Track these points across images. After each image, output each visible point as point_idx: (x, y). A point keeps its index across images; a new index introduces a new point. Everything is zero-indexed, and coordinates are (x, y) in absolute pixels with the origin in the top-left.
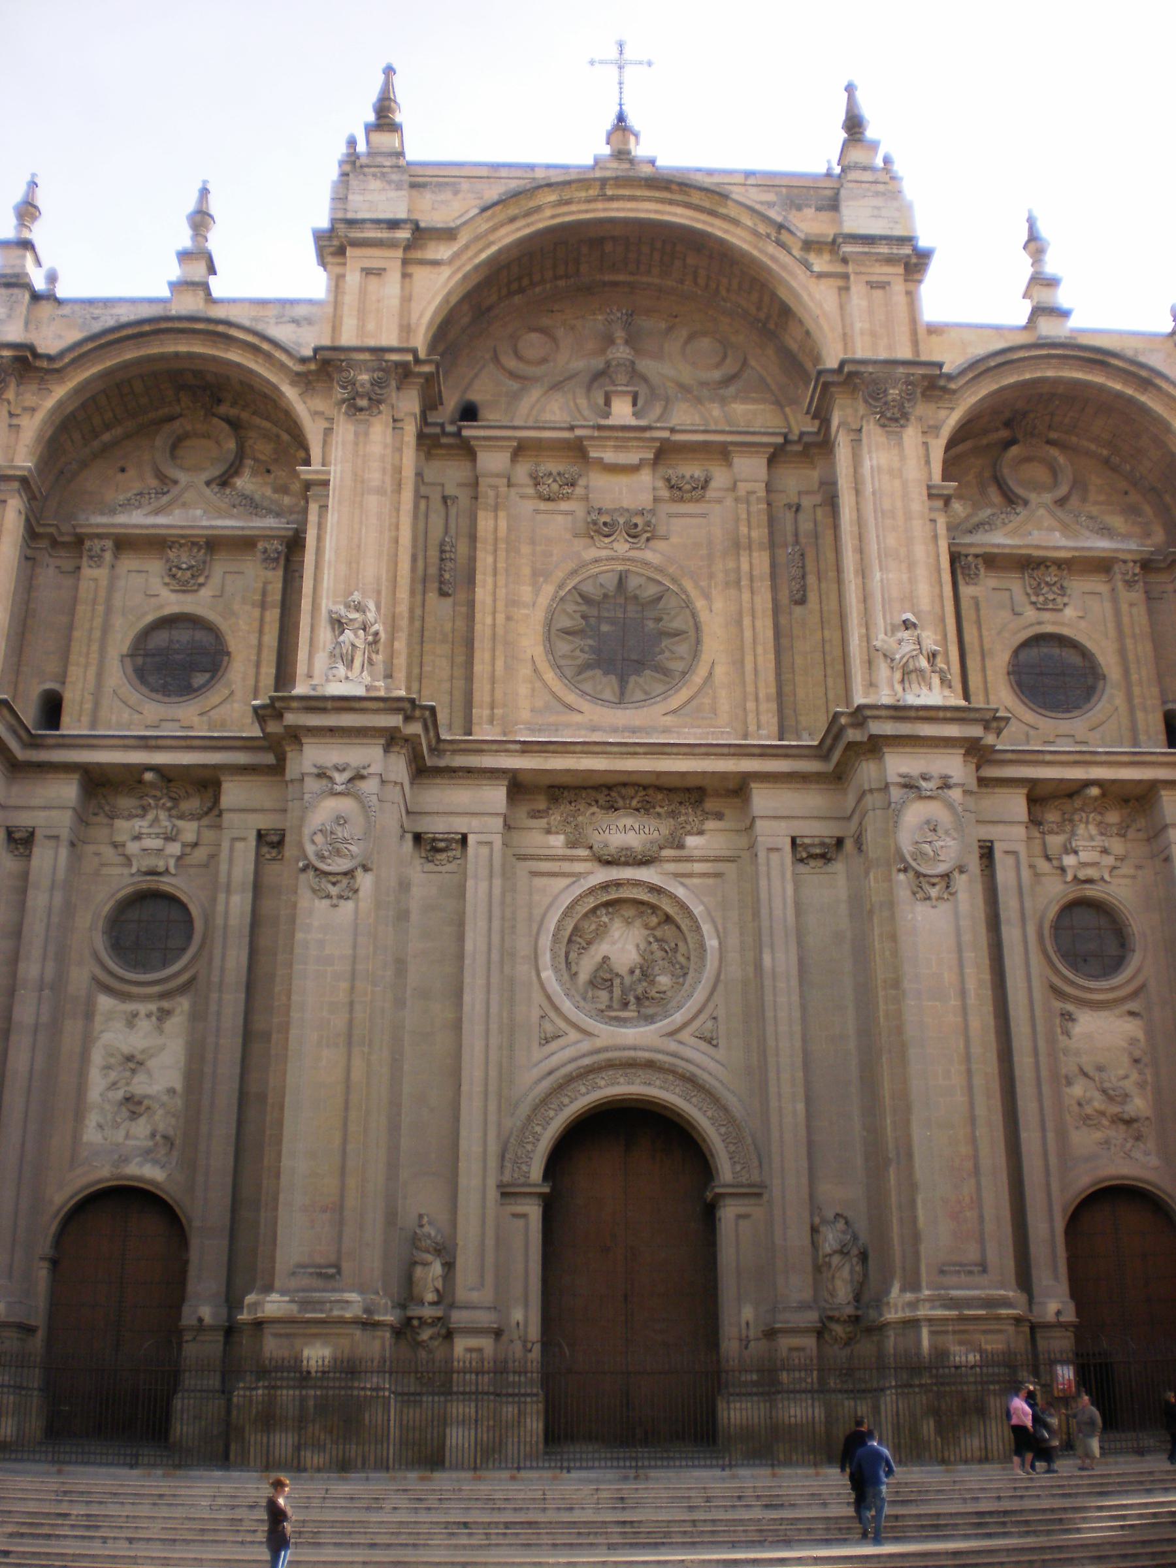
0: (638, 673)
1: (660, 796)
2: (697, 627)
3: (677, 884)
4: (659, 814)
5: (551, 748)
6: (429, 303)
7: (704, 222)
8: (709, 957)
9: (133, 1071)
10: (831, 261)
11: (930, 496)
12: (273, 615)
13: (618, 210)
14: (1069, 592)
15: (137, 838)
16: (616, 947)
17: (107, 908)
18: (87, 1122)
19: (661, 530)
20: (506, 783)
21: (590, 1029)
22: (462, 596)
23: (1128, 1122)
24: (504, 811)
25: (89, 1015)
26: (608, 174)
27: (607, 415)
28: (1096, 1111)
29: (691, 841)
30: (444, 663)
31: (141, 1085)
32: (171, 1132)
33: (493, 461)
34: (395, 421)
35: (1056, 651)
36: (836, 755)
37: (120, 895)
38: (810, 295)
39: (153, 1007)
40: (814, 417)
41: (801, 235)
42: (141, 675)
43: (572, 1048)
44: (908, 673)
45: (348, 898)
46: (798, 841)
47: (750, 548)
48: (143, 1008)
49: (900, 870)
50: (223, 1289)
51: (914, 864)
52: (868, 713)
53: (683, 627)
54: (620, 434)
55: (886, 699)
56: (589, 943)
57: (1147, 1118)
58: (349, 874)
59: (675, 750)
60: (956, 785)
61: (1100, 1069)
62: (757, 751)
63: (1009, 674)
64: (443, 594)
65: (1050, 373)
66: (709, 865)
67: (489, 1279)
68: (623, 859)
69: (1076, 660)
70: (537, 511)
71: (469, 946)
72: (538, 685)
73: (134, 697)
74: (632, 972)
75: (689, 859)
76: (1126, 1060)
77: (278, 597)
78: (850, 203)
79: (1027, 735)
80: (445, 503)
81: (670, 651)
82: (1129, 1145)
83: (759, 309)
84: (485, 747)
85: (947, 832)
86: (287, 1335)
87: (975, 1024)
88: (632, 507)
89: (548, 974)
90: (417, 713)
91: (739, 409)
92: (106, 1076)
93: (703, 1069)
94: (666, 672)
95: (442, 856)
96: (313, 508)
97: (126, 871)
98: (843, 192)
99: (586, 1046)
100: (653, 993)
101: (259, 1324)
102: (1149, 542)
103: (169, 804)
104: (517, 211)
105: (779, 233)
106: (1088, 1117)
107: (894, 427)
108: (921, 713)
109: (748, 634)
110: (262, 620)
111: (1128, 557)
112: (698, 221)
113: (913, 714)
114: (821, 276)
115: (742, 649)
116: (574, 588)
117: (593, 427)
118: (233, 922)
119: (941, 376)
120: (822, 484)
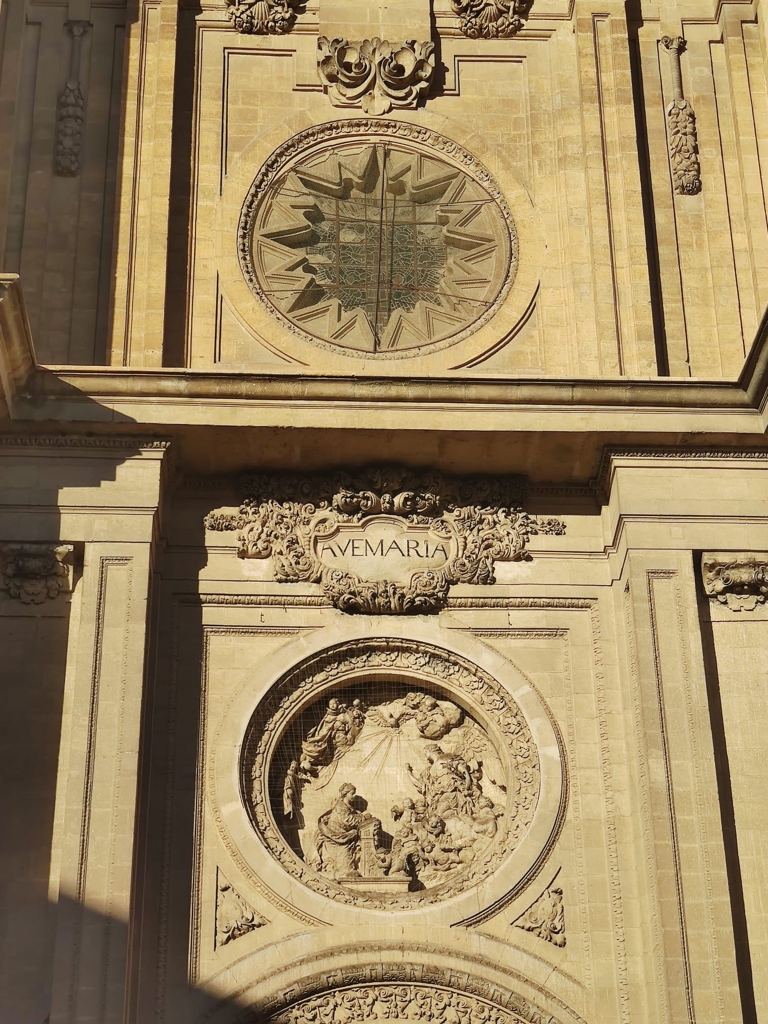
0: (408, 305)
3: (480, 647)
4: (443, 522)
5: (244, 387)
8: (543, 777)
16: (367, 770)
20: (160, 455)
24: (154, 502)
29: (503, 571)
43: (280, 946)
46: (707, 559)
53: (489, 232)
59: (473, 391)
68: (381, 600)
74: (398, 816)
80: (71, 32)
88: (396, 39)
100: (436, 853)
116: (293, 169)
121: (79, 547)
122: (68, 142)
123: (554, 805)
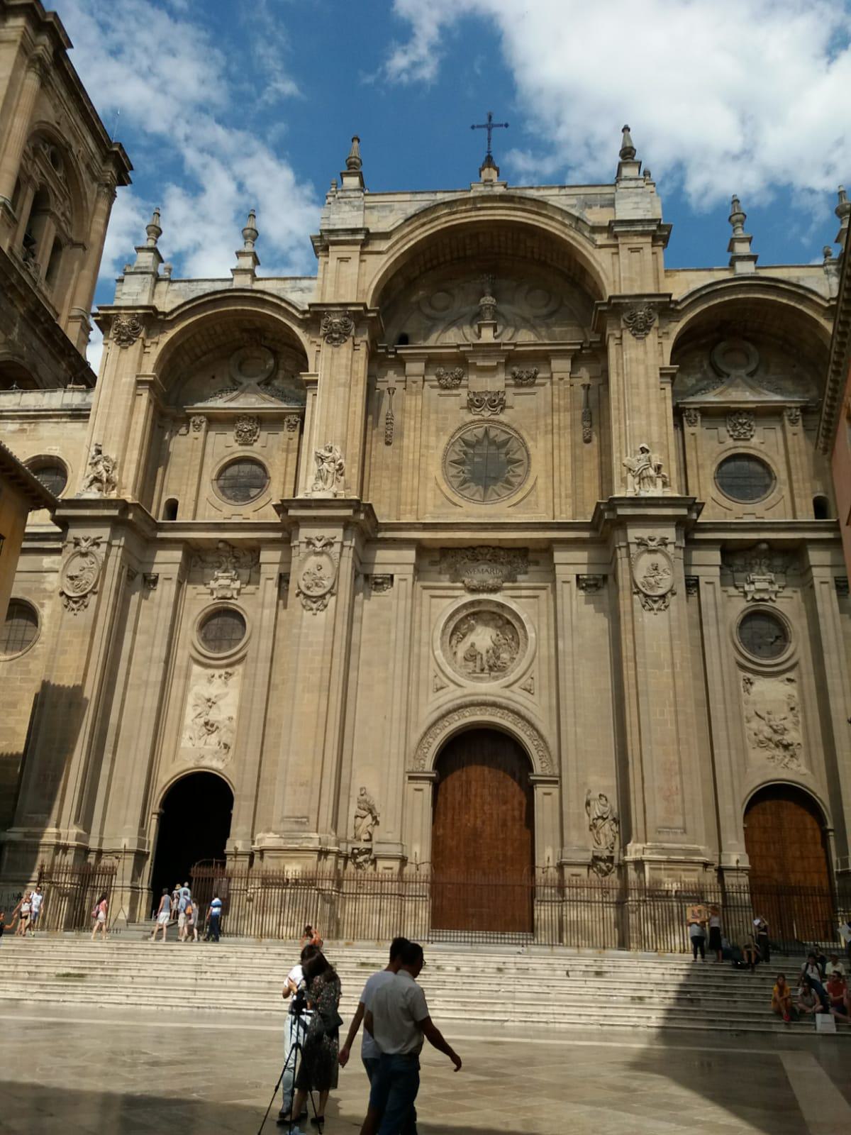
1: (502, 553)
2: (528, 455)
6: (375, 276)
7: (534, 220)
9: (210, 707)
10: (608, 238)
11: (662, 375)
12: (293, 456)
13: (484, 215)
14: (754, 428)
15: (217, 579)
17: (199, 617)
18: (183, 736)
19: (508, 403)
21: (462, 684)
22: (395, 443)
23: (786, 747)
25: (187, 676)
26: (477, 194)
27: (479, 337)
28: (766, 738)
29: (520, 577)
30: (386, 481)
31: (214, 716)
32: (228, 742)
33: (415, 368)
34: (354, 345)
35: (746, 463)
36: (601, 528)
37: (206, 611)
38: (594, 258)
39: (222, 672)
40: (596, 333)
41: (590, 224)
42: (222, 489)
44: (642, 478)
45: (322, 610)
46: (580, 577)
48: (217, 672)
49: (635, 593)
50: (250, 830)
51: (643, 589)
52: (616, 502)
53: (521, 458)
54: (486, 349)
55: (630, 494)
56: (464, 636)
57: (799, 744)
58: (323, 597)
60: (670, 543)
61: (769, 713)
62: (556, 526)
63: (715, 478)
64: (388, 443)
65: (741, 296)
66: (531, 591)
67: (398, 826)
69: (759, 469)
70: (440, 395)
71: (393, 636)
72: (439, 492)
73: (218, 502)
74: (488, 652)
76: (786, 709)
77: (296, 446)
78: (621, 201)
79: (725, 514)
81: (514, 472)
82: (786, 760)
83: (569, 270)
84: (403, 526)
85: (664, 571)
86: (277, 857)
87: (679, 682)
89: (438, 653)
90: (362, 509)
91: (557, 330)
92: (195, 710)
93: (526, 707)
95: (381, 587)
96: (310, 395)
97: (211, 598)
98: (616, 195)
99: (459, 692)
100: (499, 663)
101: (262, 852)
102: (806, 395)
103: (234, 560)
104: (425, 220)
105: (577, 223)
106: (761, 742)
107: (641, 335)
108: (649, 502)
109: (556, 461)
110: (287, 459)
111: (793, 405)
112: (529, 219)
113: (643, 502)
114: (601, 247)
117: (469, 345)
118: (265, 623)
119: (671, 302)
120: (602, 371)
121: (392, 576)
122: (389, 432)
123: (532, 653)
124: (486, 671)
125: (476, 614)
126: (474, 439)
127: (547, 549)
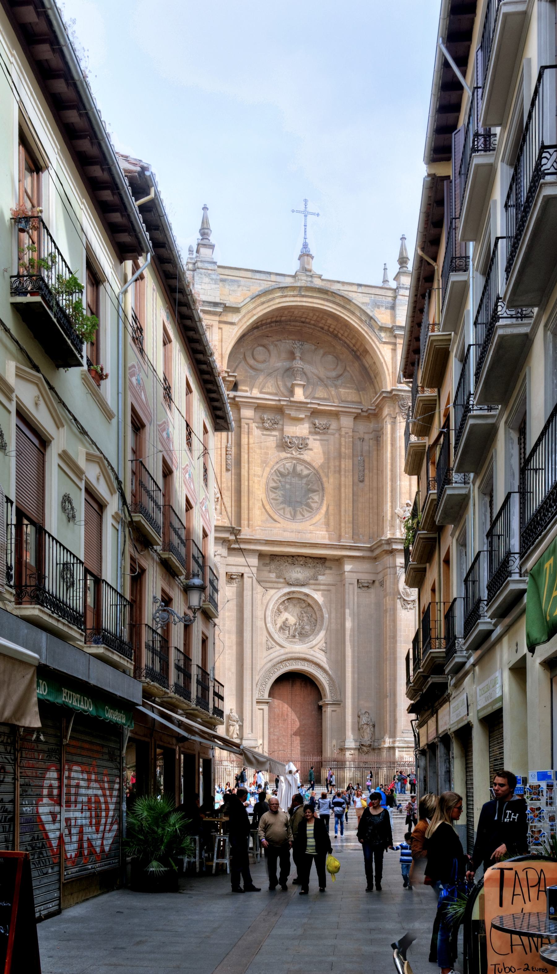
1: (311, 560)
27: (293, 397)
29: (320, 578)
36: (377, 552)
46: (359, 581)
47: (345, 459)
59: (320, 546)
70: (263, 435)
72: (263, 510)
75: (319, 584)
83: (354, 346)
91: (342, 390)
94: (310, 507)
99: (282, 651)
109: (343, 495)
115: (340, 500)
122: (229, 462)
124: (297, 637)
125: (290, 599)
126: (286, 472)
127: (339, 561)
